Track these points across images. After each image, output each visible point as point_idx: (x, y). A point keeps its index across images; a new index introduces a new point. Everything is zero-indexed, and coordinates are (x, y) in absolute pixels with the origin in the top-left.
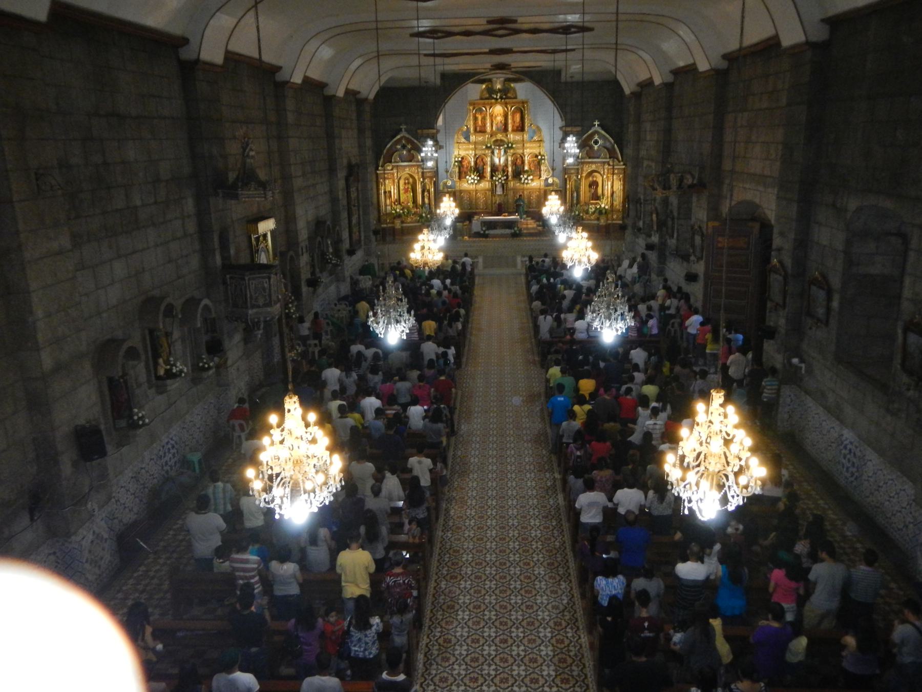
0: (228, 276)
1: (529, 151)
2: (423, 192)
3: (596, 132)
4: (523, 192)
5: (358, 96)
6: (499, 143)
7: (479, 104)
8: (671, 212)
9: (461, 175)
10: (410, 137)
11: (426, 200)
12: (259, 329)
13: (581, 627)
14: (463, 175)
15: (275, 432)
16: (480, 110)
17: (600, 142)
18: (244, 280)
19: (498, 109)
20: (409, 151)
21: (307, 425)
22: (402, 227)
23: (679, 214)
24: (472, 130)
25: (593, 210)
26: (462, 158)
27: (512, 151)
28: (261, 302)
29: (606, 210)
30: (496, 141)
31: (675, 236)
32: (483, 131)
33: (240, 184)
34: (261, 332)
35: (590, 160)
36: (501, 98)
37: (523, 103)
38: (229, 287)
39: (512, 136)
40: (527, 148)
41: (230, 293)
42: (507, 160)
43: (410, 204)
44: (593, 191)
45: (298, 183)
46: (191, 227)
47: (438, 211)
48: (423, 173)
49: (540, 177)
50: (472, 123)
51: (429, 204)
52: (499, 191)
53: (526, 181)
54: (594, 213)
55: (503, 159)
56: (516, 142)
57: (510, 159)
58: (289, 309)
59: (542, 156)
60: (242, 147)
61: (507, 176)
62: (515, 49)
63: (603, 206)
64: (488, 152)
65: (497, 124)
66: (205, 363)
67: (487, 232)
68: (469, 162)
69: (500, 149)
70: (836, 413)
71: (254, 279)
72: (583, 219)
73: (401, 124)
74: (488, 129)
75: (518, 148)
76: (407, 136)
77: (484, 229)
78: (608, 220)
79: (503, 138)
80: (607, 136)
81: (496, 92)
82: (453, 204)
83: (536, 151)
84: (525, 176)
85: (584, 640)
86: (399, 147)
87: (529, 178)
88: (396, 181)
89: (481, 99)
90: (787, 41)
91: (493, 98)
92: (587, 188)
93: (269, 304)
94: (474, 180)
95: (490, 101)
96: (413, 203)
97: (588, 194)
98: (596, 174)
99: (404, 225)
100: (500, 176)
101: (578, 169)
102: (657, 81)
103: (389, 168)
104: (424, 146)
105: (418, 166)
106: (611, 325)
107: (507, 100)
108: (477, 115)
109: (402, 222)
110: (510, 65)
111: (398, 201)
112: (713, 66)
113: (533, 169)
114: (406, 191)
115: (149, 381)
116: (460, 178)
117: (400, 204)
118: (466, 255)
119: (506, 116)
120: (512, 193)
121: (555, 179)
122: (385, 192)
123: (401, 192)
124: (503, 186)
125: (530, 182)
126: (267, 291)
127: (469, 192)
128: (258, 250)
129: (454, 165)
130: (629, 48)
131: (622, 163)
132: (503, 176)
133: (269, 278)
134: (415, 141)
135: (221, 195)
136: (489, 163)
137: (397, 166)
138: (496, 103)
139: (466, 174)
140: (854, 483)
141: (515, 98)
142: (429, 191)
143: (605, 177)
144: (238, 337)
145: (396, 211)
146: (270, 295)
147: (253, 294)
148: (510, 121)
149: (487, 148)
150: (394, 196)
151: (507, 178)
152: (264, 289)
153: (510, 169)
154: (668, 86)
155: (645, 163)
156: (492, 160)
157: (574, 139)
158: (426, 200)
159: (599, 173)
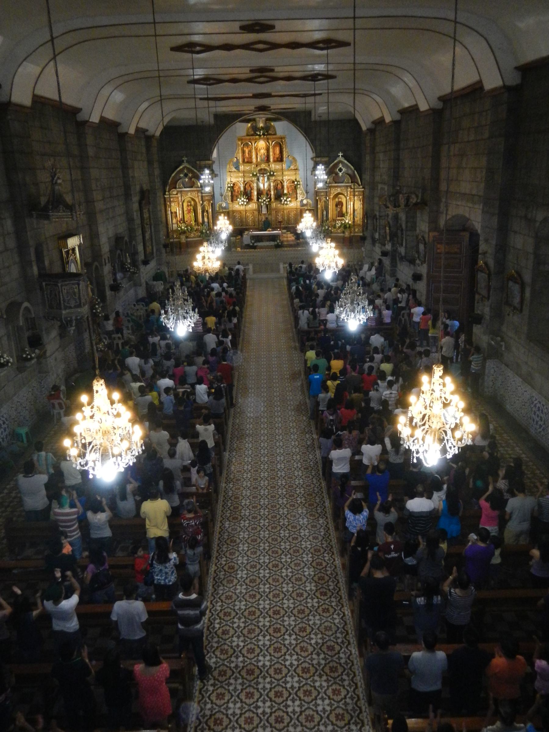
0: (44, 284)
1: (287, 178)
2: (203, 212)
3: (340, 162)
4: (283, 212)
5: (147, 133)
6: (263, 172)
7: (245, 140)
8: (401, 226)
9: (233, 198)
10: (191, 167)
11: (206, 220)
12: (71, 326)
13: (335, 552)
14: (235, 198)
15: (87, 410)
16: (247, 145)
17: (344, 170)
18: (58, 286)
19: (262, 144)
20: (190, 179)
21: (112, 403)
22: (187, 241)
23: (407, 227)
24: (241, 161)
25: (340, 224)
26: (234, 184)
27: (273, 178)
28: (73, 303)
29: (350, 224)
30: (261, 170)
31: (404, 244)
32: (250, 162)
33: (50, 207)
34: (74, 328)
35: (336, 185)
36: (264, 134)
37: (281, 138)
38: (45, 293)
39: (274, 166)
40: (285, 175)
41: (46, 296)
42: (270, 185)
43: (193, 223)
44: (339, 210)
45: (99, 206)
46: (11, 243)
47: (215, 228)
48: (202, 197)
49: (297, 199)
50: (240, 155)
51: (208, 222)
52: (264, 211)
53: (286, 202)
54: (340, 227)
55: (266, 185)
56: (276, 171)
57: (272, 184)
58: (96, 309)
59: (298, 182)
60: (52, 176)
61: (270, 198)
62: (273, 94)
63: (347, 221)
64: (255, 179)
65: (261, 156)
66: (28, 355)
67: (255, 244)
68: (239, 188)
69: (263, 177)
70: (528, 379)
71: (66, 285)
72: (331, 232)
73: (182, 157)
74: (254, 160)
75: (279, 176)
76: (188, 166)
78: (351, 232)
79: (266, 168)
80: (350, 165)
81: (259, 130)
82: (228, 222)
83: (293, 178)
84: (285, 199)
85: (338, 562)
86: (182, 175)
87: (288, 200)
88: (181, 203)
89: (248, 135)
90: (488, 85)
91: (257, 135)
93: (79, 306)
94: (244, 202)
95: (254, 137)
96: (195, 221)
97: (335, 212)
98: (340, 196)
99: (189, 240)
100: (264, 199)
102: (388, 119)
103: (175, 193)
104: (202, 175)
105: (198, 191)
106: (355, 316)
107: (268, 136)
108: (245, 149)
109: (187, 237)
110: (270, 107)
111: (183, 220)
112: (431, 106)
113: (290, 192)
114: (189, 211)
116: (232, 201)
117: (184, 222)
118: (239, 263)
119: (268, 150)
120: (274, 212)
121: (309, 200)
122: (171, 213)
123: (185, 212)
124: (267, 206)
125: (288, 203)
126: (77, 295)
127: (240, 212)
128: (68, 262)
129: (227, 190)
130: (366, 92)
131: (361, 187)
133: (79, 284)
134: (195, 171)
136: (255, 188)
137: (181, 191)
138: (260, 139)
139: (237, 197)
140: (542, 433)
141: (275, 134)
142: (207, 212)
143: (348, 198)
144: (54, 333)
145: (181, 229)
146: (80, 298)
148: (271, 153)
149: (253, 175)
150: (180, 216)
151: (271, 200)
152: (74, 293)
153: (272, 193)
154: (396, 123)
155: (380, 186)
156: (258, 185)
157: (323, 167)
158: (206, 220)
159: (343, 195)
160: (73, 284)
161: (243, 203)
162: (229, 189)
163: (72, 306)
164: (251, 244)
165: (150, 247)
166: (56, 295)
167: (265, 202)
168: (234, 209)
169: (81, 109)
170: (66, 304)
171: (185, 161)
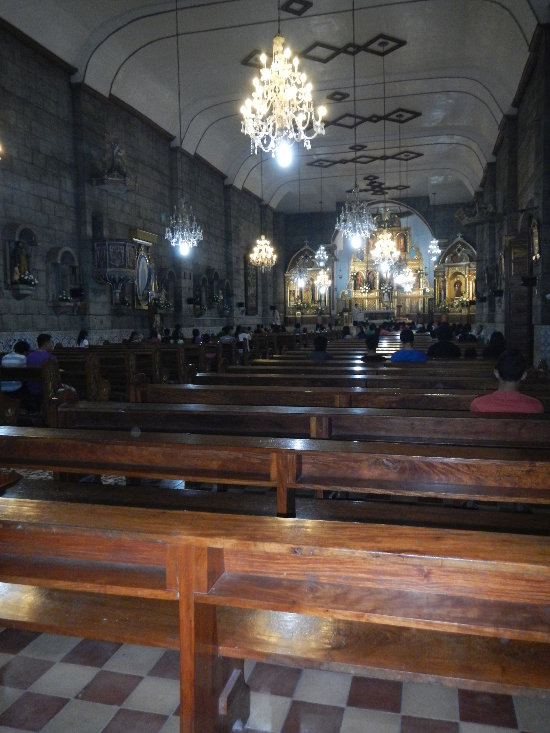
0: (96, 244)
3: (459, 242)
12: (117, 289)
14: (358, 287)
18: (105, 245)
25: (457, 303)
26: (357, 274)
35: (453, 264)
36: (388, 227)
38: (96, 253)
43: (310, 301)
44: (457, 288)
49: (420, 287)
52: (386, 298)
54: (458, 306)
59: (420, 271)
63: (464, 299)
66: (64, 296)
67: (369, 321)
68: (363, 277)
71: (113, 244)
72: (448, 312)
77: (367, 319)
78: (469, 312)
92: (453, 287)
94: (366, 290)
97: (454, 293)
101: (444, 272)
107: (393, 228)
109: (302, 314)
112: (505, 113)
115: (5, 282)
116: (355, 289)
117: (302, 299)
120: (396, 300)
126: (123, 255)
129: (351, 279)
132: (388, 287)
133: (125, 246)
135: (94, 183)
139: (360, 285)
141: (400, 226)
143: (466, 276)
145: (297, 305)
147: (111, 256)
152: (120, 254)
160: (120, 245)
161: (365, 290)
162: (352, 277)
163: (117, 265)
164: (365, 321)
165: (254, 302)
166: (103, 254)
167: (386, 290)
168: (356, 297)
169: (175, 137)
170: (111, 262)
171: (306, 244)
